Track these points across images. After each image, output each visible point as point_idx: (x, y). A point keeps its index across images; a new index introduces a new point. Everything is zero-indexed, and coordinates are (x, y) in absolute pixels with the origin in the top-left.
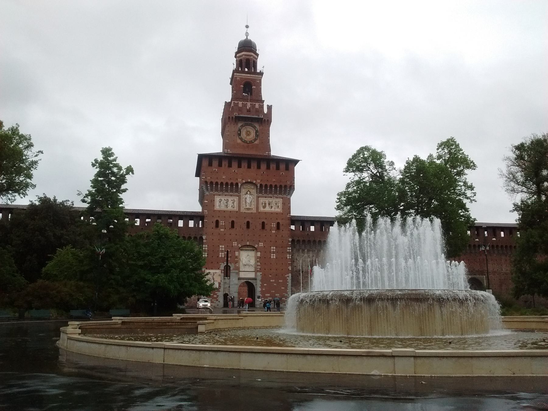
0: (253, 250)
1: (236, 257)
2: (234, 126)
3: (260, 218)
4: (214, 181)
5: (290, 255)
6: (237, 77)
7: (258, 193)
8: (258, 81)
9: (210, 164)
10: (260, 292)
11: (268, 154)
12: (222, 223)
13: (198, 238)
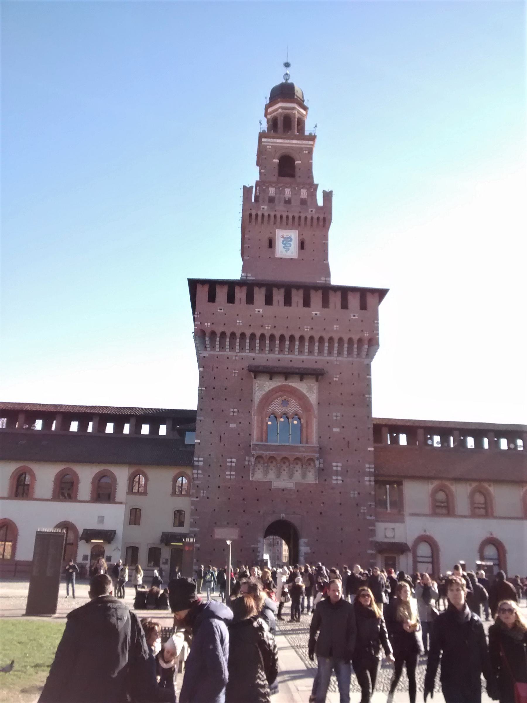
4: (219, 330)
6: (268, 145)
8: (306, 150)
9: (212, 298)
11: (326, 281)
12: (234, 412)
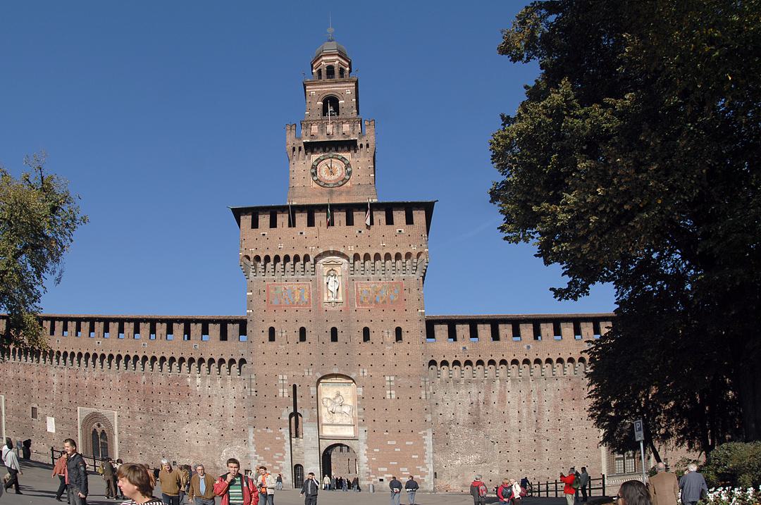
2: (305, 162)
7: (352, 272)
10: (366, 463)
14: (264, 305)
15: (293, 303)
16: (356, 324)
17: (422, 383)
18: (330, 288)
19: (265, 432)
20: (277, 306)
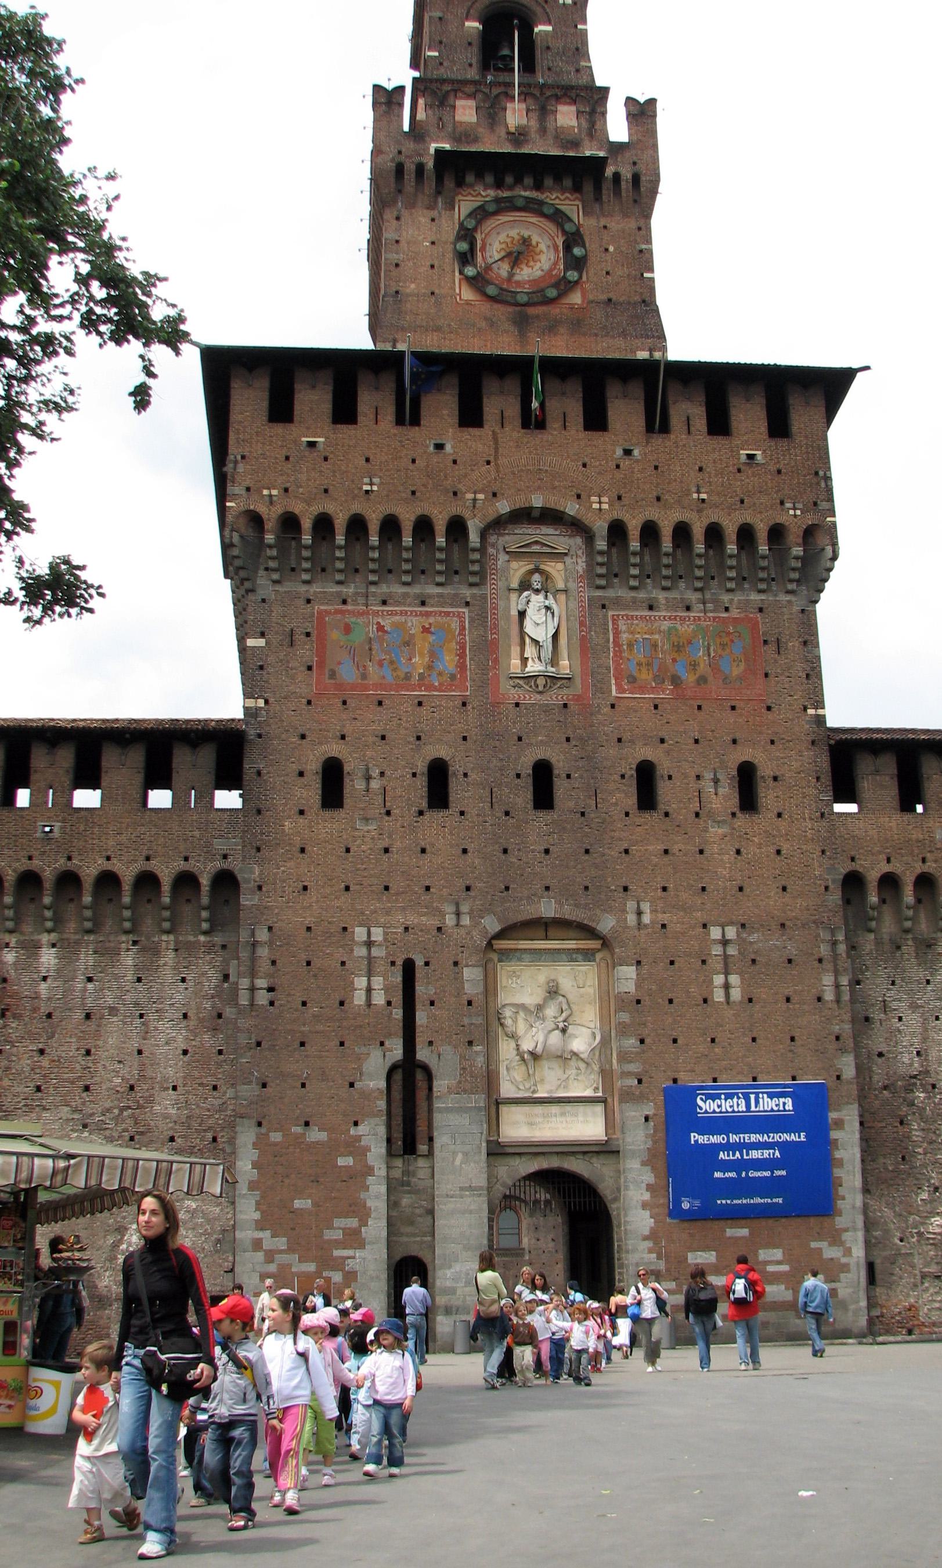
0: (588, 955)
1: (470, 1003)
3: (619, 740)
5: (844, 981)
7: (603, 582)
13: (205, 881)
14: (304, 685)
15: (408, 676)
16: (612, 751)
17: (824, 950)
18: (529, 628)
19: (298, 1141)
20: (354, 687)
